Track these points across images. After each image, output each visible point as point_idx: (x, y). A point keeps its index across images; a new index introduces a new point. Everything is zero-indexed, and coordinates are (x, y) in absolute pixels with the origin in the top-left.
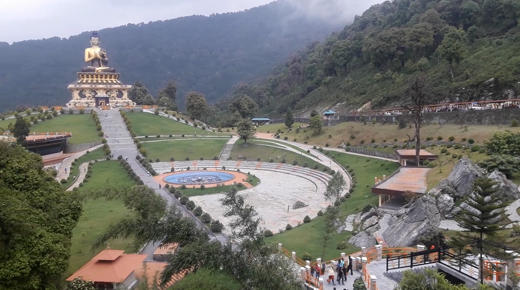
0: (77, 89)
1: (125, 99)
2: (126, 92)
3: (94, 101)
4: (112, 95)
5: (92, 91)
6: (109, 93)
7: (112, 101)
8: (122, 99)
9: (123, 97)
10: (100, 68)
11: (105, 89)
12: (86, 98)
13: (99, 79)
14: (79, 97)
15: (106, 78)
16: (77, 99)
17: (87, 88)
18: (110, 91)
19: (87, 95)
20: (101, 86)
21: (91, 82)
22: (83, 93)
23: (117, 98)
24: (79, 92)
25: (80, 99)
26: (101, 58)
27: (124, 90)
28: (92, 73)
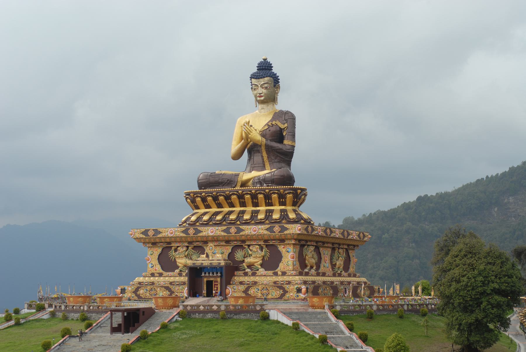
0: (154, 244)
1: (284, 274)
2: (291, 249)
3: (185, 279)
4: (248, 260)
5: (195, 248)
6: (239, 255)
7: (242, 279)
8: (276, 274)
9: (282, 267)
10: (255, 174)
11: (228, 242)
12: (177, 271)
13: (263, 208)
14: (158, 268)
15: (256, 205)
16: (153, 275)
17: (180, 240)
18: (241, 247)
19: (181, 261)
20: (209, 231)
21: (210, 219)
22: (172, 253)
23: (262, 271)
24: (159, 250)
25: (161, 275)
26: (264, 140)
27: (282, 241)
28: (214, 190)
